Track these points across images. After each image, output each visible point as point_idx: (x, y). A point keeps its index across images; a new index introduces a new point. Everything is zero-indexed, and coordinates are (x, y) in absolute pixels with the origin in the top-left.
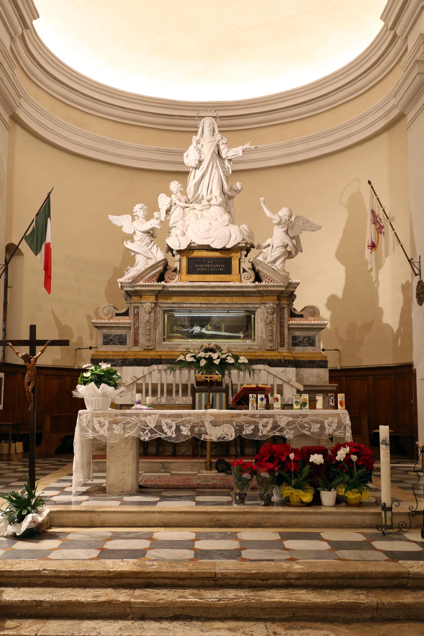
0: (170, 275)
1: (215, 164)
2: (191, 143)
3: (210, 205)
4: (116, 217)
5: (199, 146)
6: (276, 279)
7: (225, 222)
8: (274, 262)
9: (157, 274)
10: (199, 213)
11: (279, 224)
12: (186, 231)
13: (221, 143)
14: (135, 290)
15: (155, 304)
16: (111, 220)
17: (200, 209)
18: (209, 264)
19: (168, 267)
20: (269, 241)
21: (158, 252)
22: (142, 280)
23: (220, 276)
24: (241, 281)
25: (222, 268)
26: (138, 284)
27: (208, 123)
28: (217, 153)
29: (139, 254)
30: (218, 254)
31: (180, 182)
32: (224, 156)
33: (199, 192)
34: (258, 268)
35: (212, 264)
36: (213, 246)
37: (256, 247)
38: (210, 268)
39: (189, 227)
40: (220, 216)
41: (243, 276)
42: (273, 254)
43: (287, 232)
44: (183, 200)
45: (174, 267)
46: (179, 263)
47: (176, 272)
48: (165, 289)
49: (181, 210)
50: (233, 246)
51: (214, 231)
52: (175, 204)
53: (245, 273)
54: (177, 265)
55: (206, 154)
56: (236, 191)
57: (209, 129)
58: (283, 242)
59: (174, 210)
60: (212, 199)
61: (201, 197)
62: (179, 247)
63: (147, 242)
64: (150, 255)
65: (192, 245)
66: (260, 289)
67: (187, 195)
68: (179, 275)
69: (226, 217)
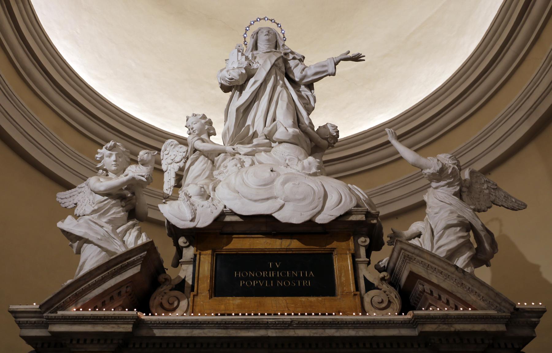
0: (166, 297)
6: (472, 298)
9: (124, 290)
10: (248, 160)
14: (54, 334)
18: (271, 270)
19: (161, 278)
24: (364, 312)
25: (308, 279)
26: (60, 313)
29: (88, 241)
30: (294, 244)
35: (280, 270)
38: (275, 279)
41: (367, 299)
45: (179, 277)
46: (191, 267)
47: (183, 291)
48: (144, 332)
49: (206, 163)
50: (333, 218)
53: (372, 293)
58: (459, 216)
59: (192, 164)
62: (193, 220)
63: (114, 216)
65: (228, 219)
68: (191, 299)
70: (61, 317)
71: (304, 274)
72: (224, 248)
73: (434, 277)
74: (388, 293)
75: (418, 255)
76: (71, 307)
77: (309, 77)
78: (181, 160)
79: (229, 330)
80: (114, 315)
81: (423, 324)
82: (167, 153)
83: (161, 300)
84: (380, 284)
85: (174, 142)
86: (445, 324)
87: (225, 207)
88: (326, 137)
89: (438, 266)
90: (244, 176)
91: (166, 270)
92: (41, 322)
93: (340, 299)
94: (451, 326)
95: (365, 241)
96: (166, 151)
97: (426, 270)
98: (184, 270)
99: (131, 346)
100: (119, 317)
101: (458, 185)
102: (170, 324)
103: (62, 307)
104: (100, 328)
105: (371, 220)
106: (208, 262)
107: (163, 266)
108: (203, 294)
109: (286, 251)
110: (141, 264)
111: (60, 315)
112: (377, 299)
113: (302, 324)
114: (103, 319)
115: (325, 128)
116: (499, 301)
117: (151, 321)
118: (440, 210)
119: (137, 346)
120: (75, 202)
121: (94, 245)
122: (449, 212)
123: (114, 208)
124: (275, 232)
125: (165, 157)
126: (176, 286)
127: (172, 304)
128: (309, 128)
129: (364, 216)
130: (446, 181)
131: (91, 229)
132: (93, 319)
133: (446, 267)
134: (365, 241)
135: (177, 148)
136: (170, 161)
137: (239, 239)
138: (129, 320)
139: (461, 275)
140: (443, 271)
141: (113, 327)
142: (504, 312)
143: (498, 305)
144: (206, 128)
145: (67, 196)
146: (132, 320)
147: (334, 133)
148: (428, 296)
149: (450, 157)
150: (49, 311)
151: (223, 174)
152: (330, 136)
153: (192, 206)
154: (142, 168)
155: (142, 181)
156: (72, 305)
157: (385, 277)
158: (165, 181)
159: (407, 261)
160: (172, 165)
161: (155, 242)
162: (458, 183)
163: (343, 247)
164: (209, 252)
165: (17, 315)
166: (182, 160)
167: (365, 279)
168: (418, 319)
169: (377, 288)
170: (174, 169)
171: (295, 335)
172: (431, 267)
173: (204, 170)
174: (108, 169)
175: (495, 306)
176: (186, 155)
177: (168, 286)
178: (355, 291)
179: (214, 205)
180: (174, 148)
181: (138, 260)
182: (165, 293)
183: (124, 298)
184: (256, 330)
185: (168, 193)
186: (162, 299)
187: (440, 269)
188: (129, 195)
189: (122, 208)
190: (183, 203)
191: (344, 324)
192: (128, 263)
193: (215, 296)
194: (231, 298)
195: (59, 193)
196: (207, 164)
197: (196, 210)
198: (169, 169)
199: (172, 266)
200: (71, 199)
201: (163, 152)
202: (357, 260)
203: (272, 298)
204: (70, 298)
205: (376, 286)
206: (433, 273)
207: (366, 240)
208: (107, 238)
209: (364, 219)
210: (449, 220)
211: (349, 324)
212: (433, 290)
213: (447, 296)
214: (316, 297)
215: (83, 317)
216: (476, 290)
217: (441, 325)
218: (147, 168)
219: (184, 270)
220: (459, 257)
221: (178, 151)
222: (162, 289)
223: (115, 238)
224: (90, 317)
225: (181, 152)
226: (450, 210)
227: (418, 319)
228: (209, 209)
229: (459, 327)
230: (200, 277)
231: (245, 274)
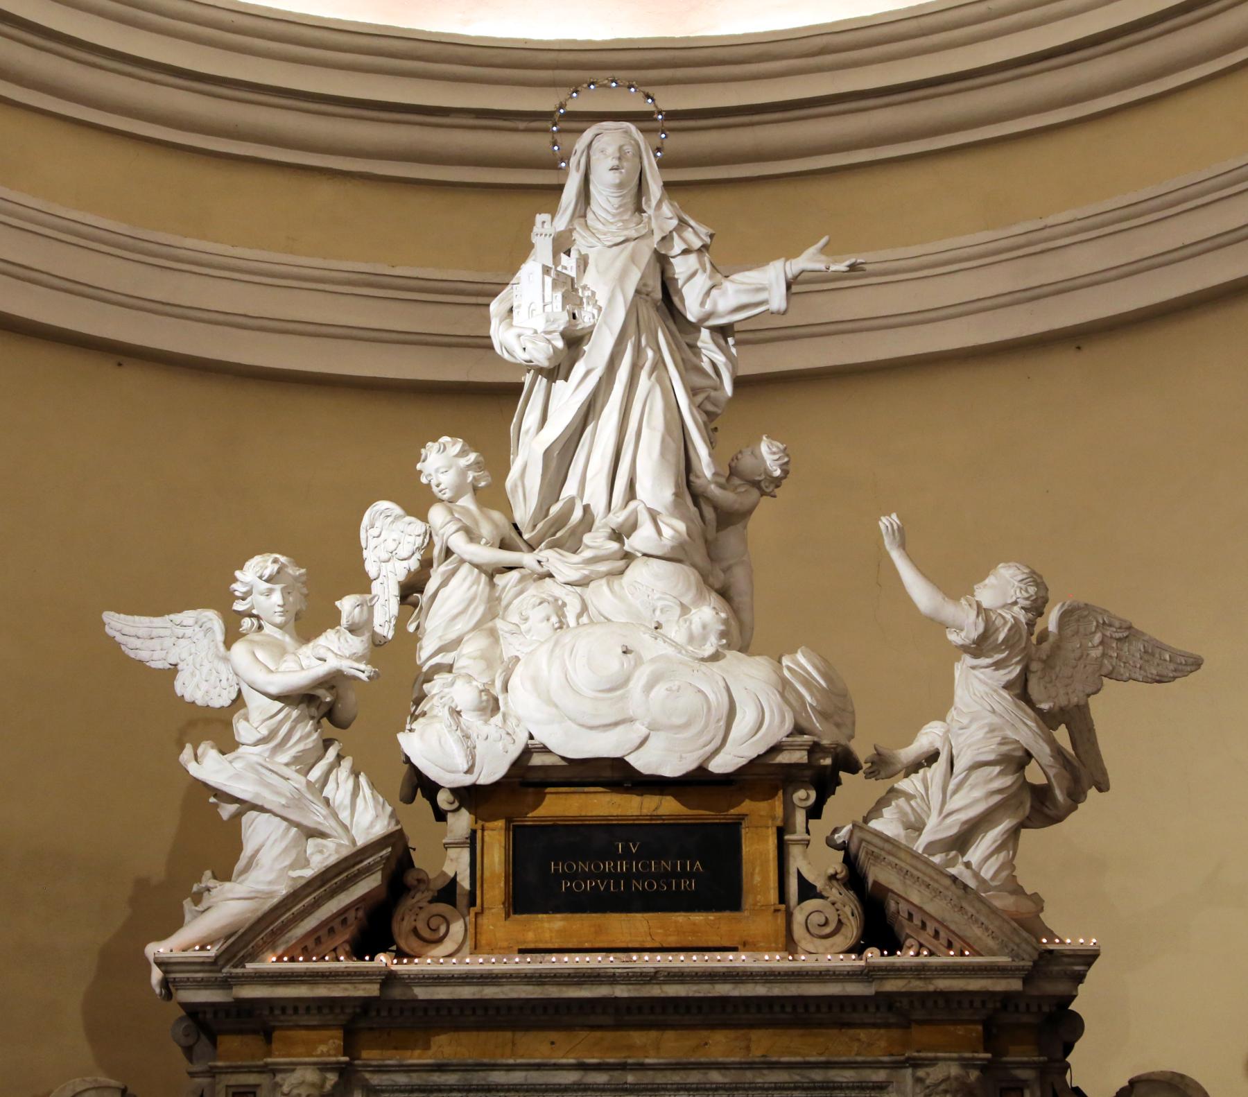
0: (423, 916)
1: (650, 353)
2: (524, 250)
3: (628, 557)
4: (145, 620)
5: (569, 264)
7: (704, 638)
8: (961, 841)
9: (351, 915)
11: (979, 647)
12: (505, 689)
13: (678, 246)
14: (239, 1002)
15: (345, 1072)
16: (119, 638)
17: (575, 575)
18: (621, 858)
19: (410, 878)
20: (929, 736)
21: (360, 801)
22: (274, 949)
23: (680, 918)
24: (790, 945)
25: (690, 876)
26: (251, 966)
27: (612, 149)
28: (658, 295)
29: (262, 809)
30: (668, 806)
31: (472, 443)
32: (692, 311)
33: (569, 489)
34: (877, 874)
35: (637, 857)
36: (644, 762)
37: (865, 766)
38: (628, 877)
39: (519, 670)
40: (678, 610)
41: (799, 917)
42: (953, 804)
43: (1021, 690)
44: (486, 530)
45: (444, 874)
46: (465, 854)
47: (453, 904)
48: (397, 993)
49: (477, 581)
50: (743, 762)
51: (649, 687)
52: (448, 553)
54: (457, 864)
55: (602, 301)
56: (756, 484)
57: (614, 177)
58: (1004, 741)
59: (444, 584)
60: (634, 527)
61: (577, 514)
62: (469, 771)
63: (301, 747)
64: (317, 816)
65: (537, 760)
66: (891, 986)
67: (507, 509)
68: (471, 918)
69: (708, 614)
70: (253, 975)
71: (683, 866)
72: (530, 815)
73: (916, 892)
74: (838, 905)
75: (889, 853)
76: (266, 954)
77: (722, 316)
78: (411, 554)
79: (547, 987)
80: (348, 970)
81: (882, 979)
82: (376, 535)
83: (414, 923)
84: (827, 887)
86: (921, 978)
87: (531, 737)
88: (758, 478)
89: (924, 874)
90: (567, 663)
91: (411, 851)
92: (213, 979)
93: (748, 917)
94: (930, 983)
95: (807, 798)
97: (902, 878)
98: (452, 860)
99: (373, 1013)
100: (355, 972)
101: (1017, 663)
102: (443, 978)
103: (250, 955)
104: (322, 991)
105: (821, 758)
106: (500, 846)
107: (407, 846)
108: (493, 911)
109: (651, 820)
111: (251, 971)
112: (817, 919)
113: (674, 976)
114: (328, 976)
115: (756, 457)
116: (1017, 940)
117: (409, 975)
118: (971, 722)
119: (384, 1013)
121: (273, 816)
122: (986, 729)
124: (630, 785)
126: (440, 891)
127: (436, 930)
128: (713, 486)
129: (805, 753)
130: (991, 657)
131: (268, 785)
132: (310, 976)
133: (936, 877)
134: (807, 798)
135: (401, 524)
136: (385, 556)
137: (558, 795)
138: (374, 977)
139: (960, 892)
140: (931, 883)
141: (346, 990)
142: (1023, 959)
143: (1015, 948)
144: (470, 479)
145: (140, 633)
147: (776, 470)
148: (905, 922)
149: (1023, 580)
150: (232, 964)
151: (520, 636)
152: (765, 478)
153: (466, 740)
154: (352, 640)
155: (355, 678)
156: (266, 951)
157: (836, 873)
159: (871, 861)
160: (390, 565)
161: (406, 831)
162: (1018, 658)
163: (763, 813)
164: (501, 823)
166: (413, 554)
167: (800, 877)
168: (874, 971)
169: (822, 897)
171: (663, 995)
172: (912, 875)
173: (472, 600)
174: (262, 615)
175: (1010, 949)
176: (423, 542)
177: (426, 894)
178: (777, 902)
179: (508, 734)
180: (393, 522)
181: (376, 863)
182: (421, 908)
183: (352, 928)
184: (595, 987)
185: (385, 634)
186: (415, 920)
187: (927, 879)
188: (328, 699)
189: (311, 722)
190: (446, 731)
191: (749, 976)
192: (358, 870)
193: (515, 913)
194: (545, 916)
195: (112, 613)
196: (479, 584)
197: (475, 748)
198: (383, 573)
200: (155, 643)
201: (367, 531)
202: (787, 837)
203: (623, 916)
204: (262, 938)
205: (818, 890)
206: (915, 886)
207: (808, 794)
208: (297, 801)
209: (805, 760)
210: (981, 751)
211: (757, 975)
212: (914, 913)
213: (936, 925)
214: (704, 914)
215: (293, 973)
216: (983, 919)
217: (913, 981)
218: (360, 638)
219: (452, 860)
220: (987, 832)
222: (415, 900)
223: (315, 801)
224: (305, 973)
226: (990, 724)
227: (874, 971)
228: (501, 743)
229: (943, 984)
230: (485, 877)
231: (570, 867)
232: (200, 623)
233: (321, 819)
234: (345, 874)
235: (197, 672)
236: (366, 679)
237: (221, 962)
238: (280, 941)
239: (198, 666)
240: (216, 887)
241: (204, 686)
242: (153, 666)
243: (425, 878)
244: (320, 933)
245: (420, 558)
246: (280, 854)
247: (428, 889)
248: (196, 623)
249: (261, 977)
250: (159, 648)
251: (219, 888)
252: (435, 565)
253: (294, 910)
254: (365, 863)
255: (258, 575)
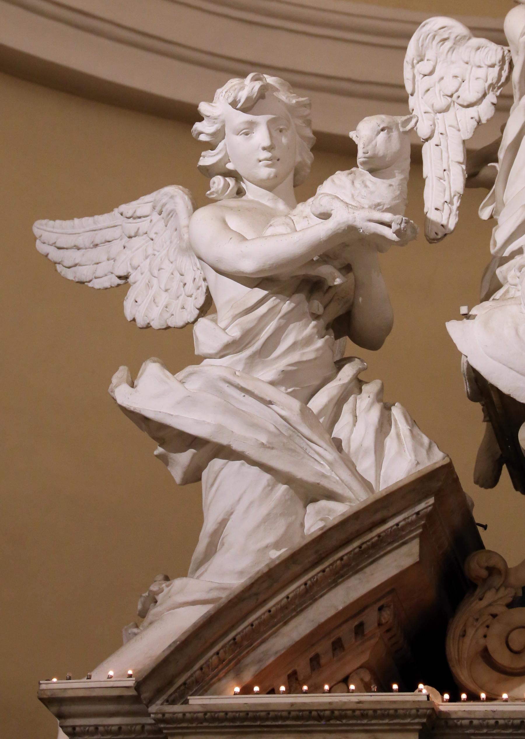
4: (88, 222)
16: (54, 255)
21: (390, 442)
22: (238, 674)
63: (295, 357)
70: (201, 715)
76: (224, 681)
78: (480, 95)
80: (361, 706)
82: (427, 72)
83: (482, 641)
85: (451, 27)
91: (480, 529)
92: (138, 728)
96: (422, 60)
100: (375, 711)
103: (197, 682)
107: (472, 519)
110: (421, 535)
111: (200, 709)
114: (329, 719)
120: (122, 273)
121: (247, 465)
123: (292, 326)
125: (422, 84)
132: (297, 718)
136: (443, 102)
138: (408, 721)
145: (80, 241)
146: (417, 721)
150: (165, 697)
154: (375, 183)
155: (383, 238)
156: (225, 676)
158: (429, 175)
160: (449, 115)
165: (66, 709)
166: (484, 95)
170: (459, 130)
174: (241, 172)
176: (500, 76)
177: (502, 592)
180: (452, 49)
182: (494, 616)
183: (373, 641)
185: (444, 222)
186: (485, 636)
189: (314, 323)
192: (379, 536)
195: (44, 221)
198: (439, 129)
199: (476, 482)
200: (100, 253)
201: (413, 67)
204: (217, 653)
218: (389, 181)
221: (467, 63)
223: (315, 438)
224: (289, 712)
225: (479, 67)
232: (158, 208)
233: (326, 470)
234: (356, 544)
235: (155, 281)
236: (394, 237)
237: (146, 695)
238: (249, 659)
239: (155, 272)
240: (161, 591)
241: (163, 299)
242: (97, 286)
243: (500, 566)
244: (319, 649)
245: (495, 101)
246: (258, 526)
247: (505, 585)
248: (154, 208)
249: (213, 719)
250: (105, 258)
251: (166, 590)
252: (516, 100)
253: (271, 604)
254: (391, 523)
255: (230, 100)
